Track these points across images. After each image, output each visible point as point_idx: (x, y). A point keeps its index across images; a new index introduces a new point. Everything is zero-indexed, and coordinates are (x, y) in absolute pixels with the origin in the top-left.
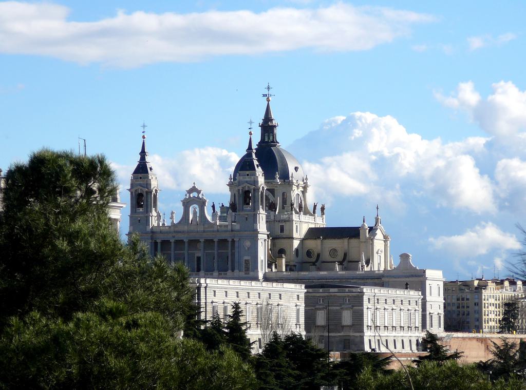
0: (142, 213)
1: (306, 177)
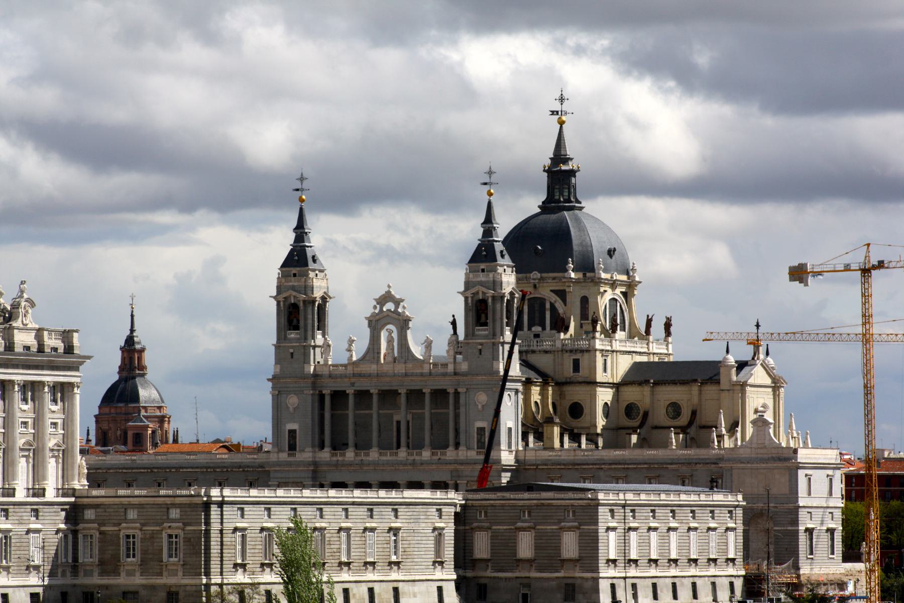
0: (297, 340)
1: (633, 267)
